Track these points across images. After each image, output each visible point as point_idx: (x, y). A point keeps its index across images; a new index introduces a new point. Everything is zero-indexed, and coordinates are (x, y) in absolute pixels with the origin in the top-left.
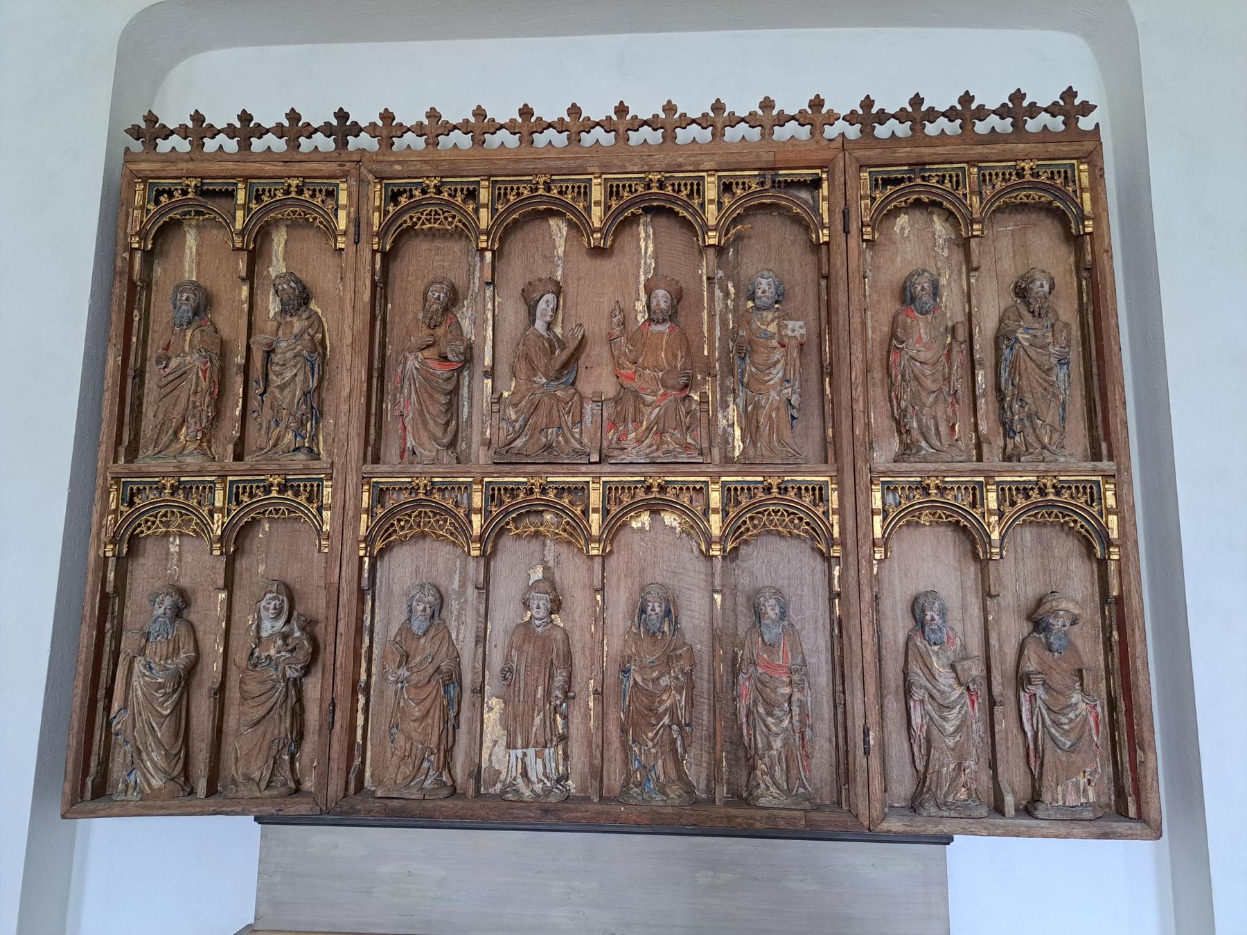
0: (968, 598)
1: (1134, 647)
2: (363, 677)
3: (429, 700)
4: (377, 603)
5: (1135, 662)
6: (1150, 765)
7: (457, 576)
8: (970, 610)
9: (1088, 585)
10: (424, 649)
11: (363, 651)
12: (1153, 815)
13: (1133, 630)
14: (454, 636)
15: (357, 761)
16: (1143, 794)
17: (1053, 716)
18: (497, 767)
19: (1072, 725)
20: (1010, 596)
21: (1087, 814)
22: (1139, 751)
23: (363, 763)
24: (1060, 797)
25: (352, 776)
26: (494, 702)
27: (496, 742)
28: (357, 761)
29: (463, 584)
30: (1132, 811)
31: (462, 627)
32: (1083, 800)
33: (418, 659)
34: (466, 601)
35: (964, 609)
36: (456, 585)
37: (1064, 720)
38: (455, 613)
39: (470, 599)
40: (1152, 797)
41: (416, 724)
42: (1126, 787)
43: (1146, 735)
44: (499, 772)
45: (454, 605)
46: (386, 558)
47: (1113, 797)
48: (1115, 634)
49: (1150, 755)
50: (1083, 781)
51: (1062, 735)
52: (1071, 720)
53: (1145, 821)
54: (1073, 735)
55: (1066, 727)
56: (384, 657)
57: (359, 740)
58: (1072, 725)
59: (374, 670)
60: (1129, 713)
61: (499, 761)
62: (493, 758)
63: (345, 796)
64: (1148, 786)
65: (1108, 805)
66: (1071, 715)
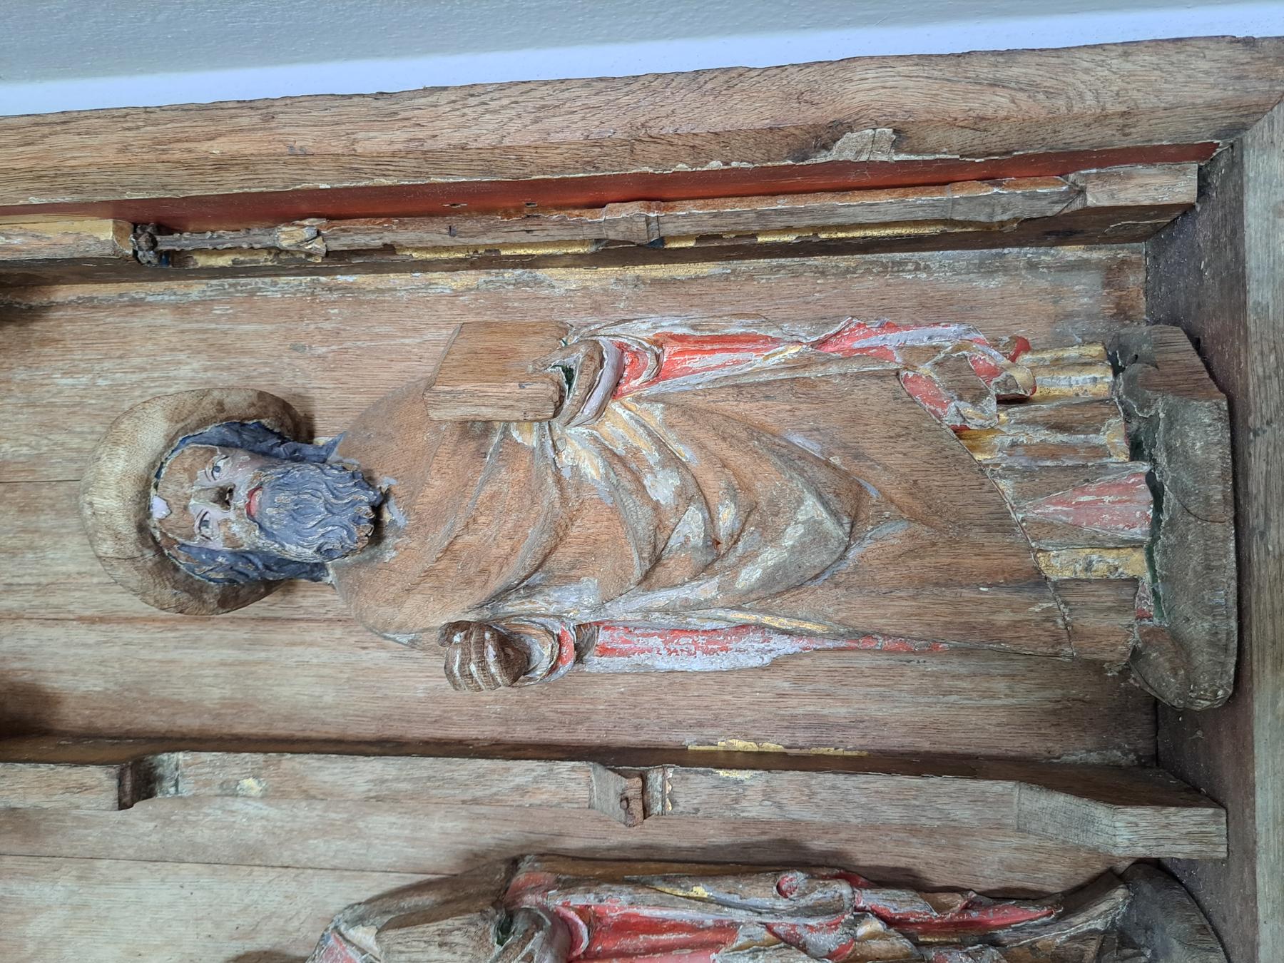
0: (203, 835)
1: (302, 157)
5: (380, 162)
6: (913, 96)
8: (255, 834)
9: (138, 322)
12: (1198, 91)
13: (221, 165)
16: (1074, 137)
17: (675, 567)
19: (714, 484)
20: (192, 657)
21: (1202, 433)
22: (844, 150)
24: (1104, 561)
30: (1175, 186)
32: (1113, 436)
35: (246, 857)
37: (691, 525)
40: (1089, 98)
42: (1024, 209)
43: (750, 114)
47: (1072, 252)
48: (287, 236)
49: (860, 93)
50: (1010, 430)
51: (770, 534)
52: (693, 493)
53: (1235, 132)
54: (769, 480)
55: (727, 516)
58: (714, 484)
60: (656, 190)
64: (1035, 107)
65: (1112, 274)
66: (663, 487)
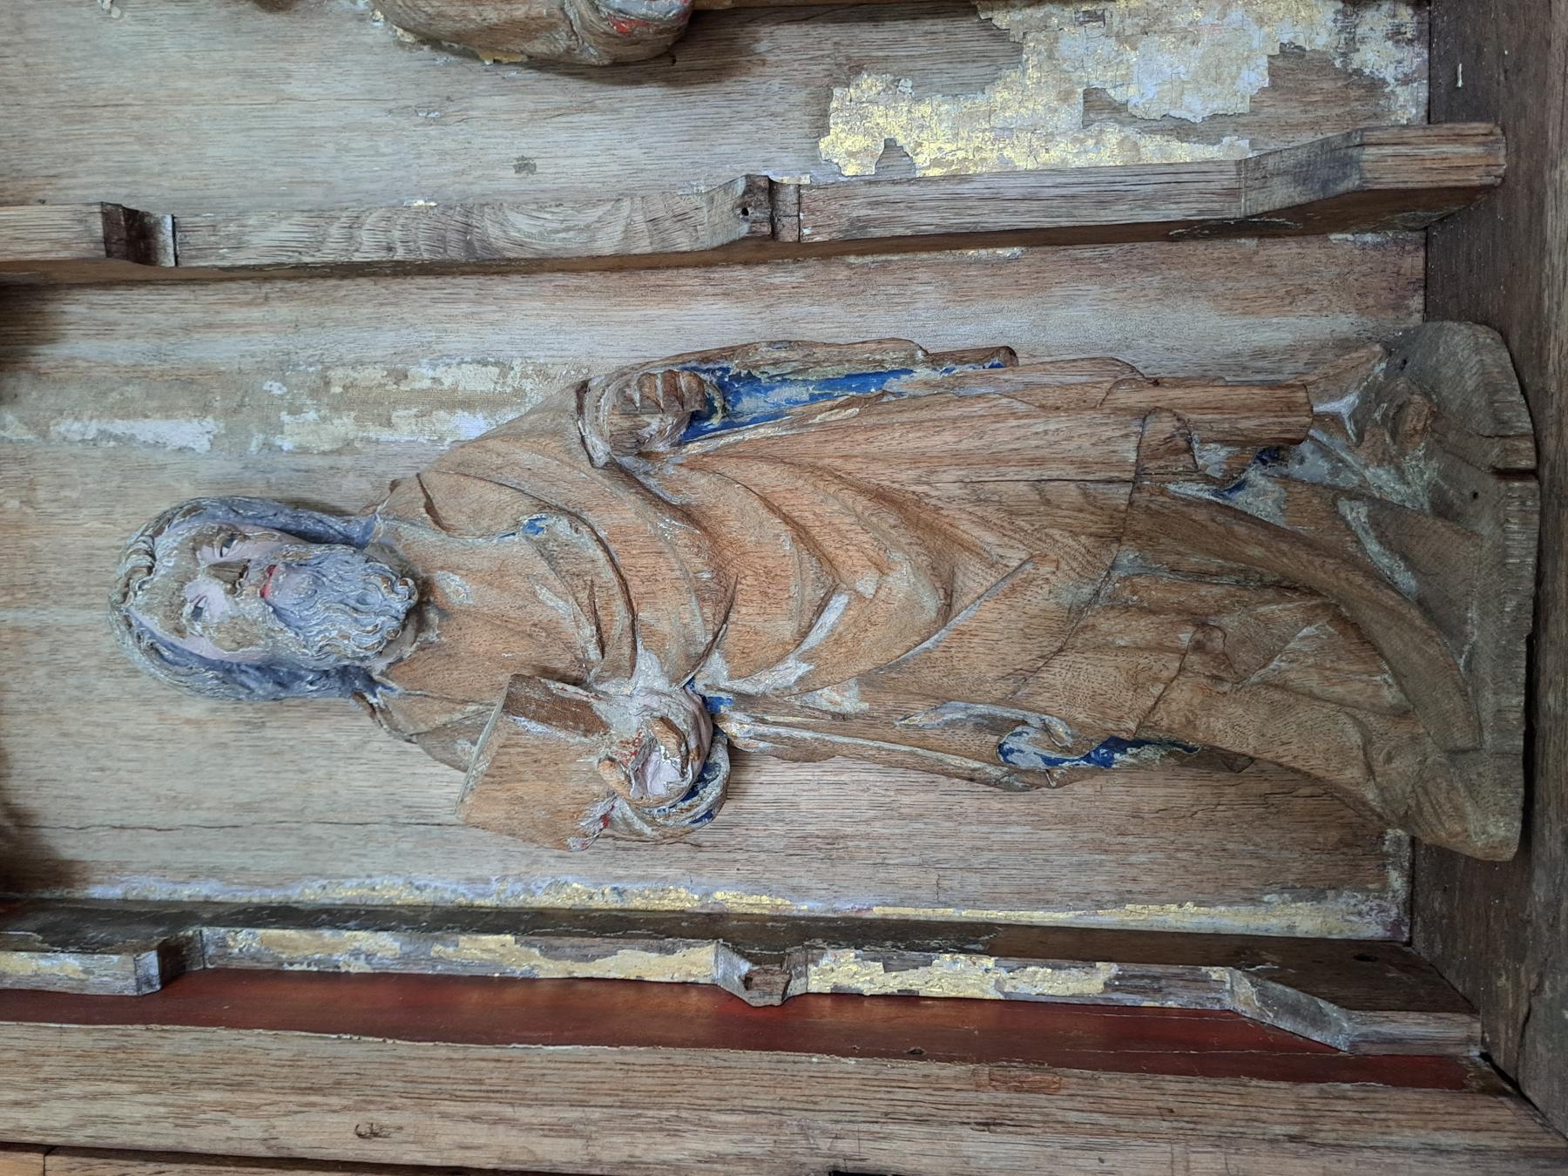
2: (701, 962)
3: (810, 502)
4: (309, 893)
7: (147, 429)
10: (497, 576)
11: (550, 969)
14: (471, 425)
15: (1236, 992)
18: (1255, 77)
23: (1239, 951)
25: (1341, 1029)
26: (847, 147)
27: (1098, 106)
28: (1236, 992)
29: (191, 389)
31: (422, 376)
33: (557, 605)
34: (282, 366)
36: (189, 432)
38: (344, 425)
39: (265, 343)
41: (974, 579)
44: (1291, 65)
45: (306, 433)
46: (69, 848)
56: (553, 832)
57: (1085, 983)
59: (683, 898)
61: (1215, 73)
62: (1195, 108)
63: (1504, 1083)
